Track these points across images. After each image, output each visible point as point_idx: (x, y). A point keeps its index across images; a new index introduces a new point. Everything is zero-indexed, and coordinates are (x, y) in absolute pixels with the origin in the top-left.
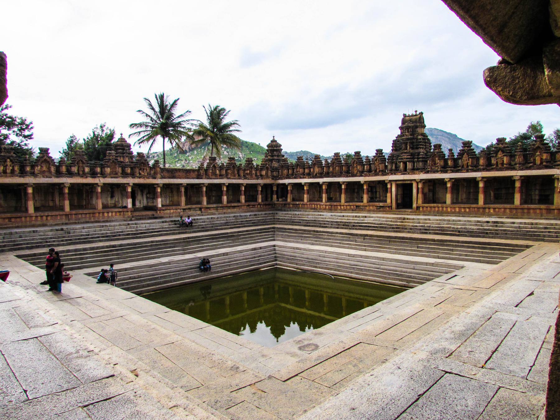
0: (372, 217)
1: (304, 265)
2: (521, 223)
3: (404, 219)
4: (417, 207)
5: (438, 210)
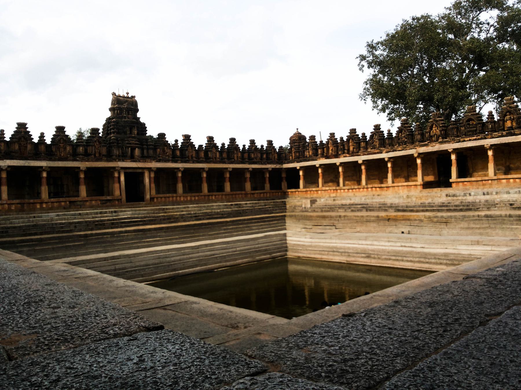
0: (125, 211)
1: (156, 273)
2: (250, 204)
3: (164, 209)
4: (151, 198)
5: (173, 201)
